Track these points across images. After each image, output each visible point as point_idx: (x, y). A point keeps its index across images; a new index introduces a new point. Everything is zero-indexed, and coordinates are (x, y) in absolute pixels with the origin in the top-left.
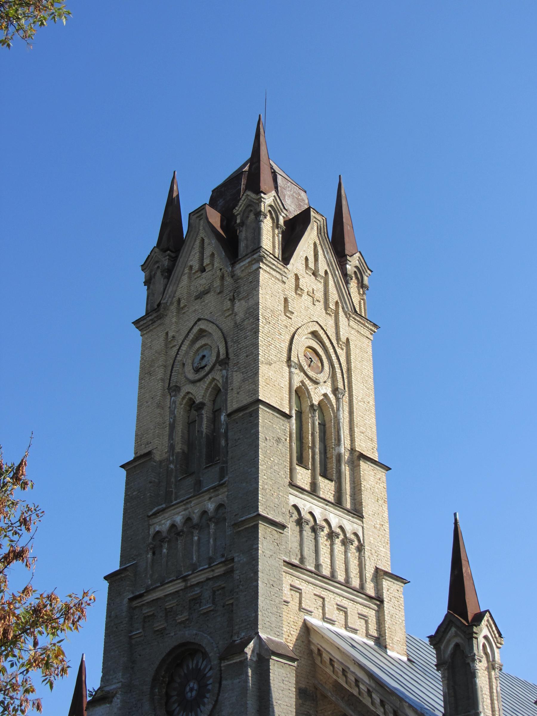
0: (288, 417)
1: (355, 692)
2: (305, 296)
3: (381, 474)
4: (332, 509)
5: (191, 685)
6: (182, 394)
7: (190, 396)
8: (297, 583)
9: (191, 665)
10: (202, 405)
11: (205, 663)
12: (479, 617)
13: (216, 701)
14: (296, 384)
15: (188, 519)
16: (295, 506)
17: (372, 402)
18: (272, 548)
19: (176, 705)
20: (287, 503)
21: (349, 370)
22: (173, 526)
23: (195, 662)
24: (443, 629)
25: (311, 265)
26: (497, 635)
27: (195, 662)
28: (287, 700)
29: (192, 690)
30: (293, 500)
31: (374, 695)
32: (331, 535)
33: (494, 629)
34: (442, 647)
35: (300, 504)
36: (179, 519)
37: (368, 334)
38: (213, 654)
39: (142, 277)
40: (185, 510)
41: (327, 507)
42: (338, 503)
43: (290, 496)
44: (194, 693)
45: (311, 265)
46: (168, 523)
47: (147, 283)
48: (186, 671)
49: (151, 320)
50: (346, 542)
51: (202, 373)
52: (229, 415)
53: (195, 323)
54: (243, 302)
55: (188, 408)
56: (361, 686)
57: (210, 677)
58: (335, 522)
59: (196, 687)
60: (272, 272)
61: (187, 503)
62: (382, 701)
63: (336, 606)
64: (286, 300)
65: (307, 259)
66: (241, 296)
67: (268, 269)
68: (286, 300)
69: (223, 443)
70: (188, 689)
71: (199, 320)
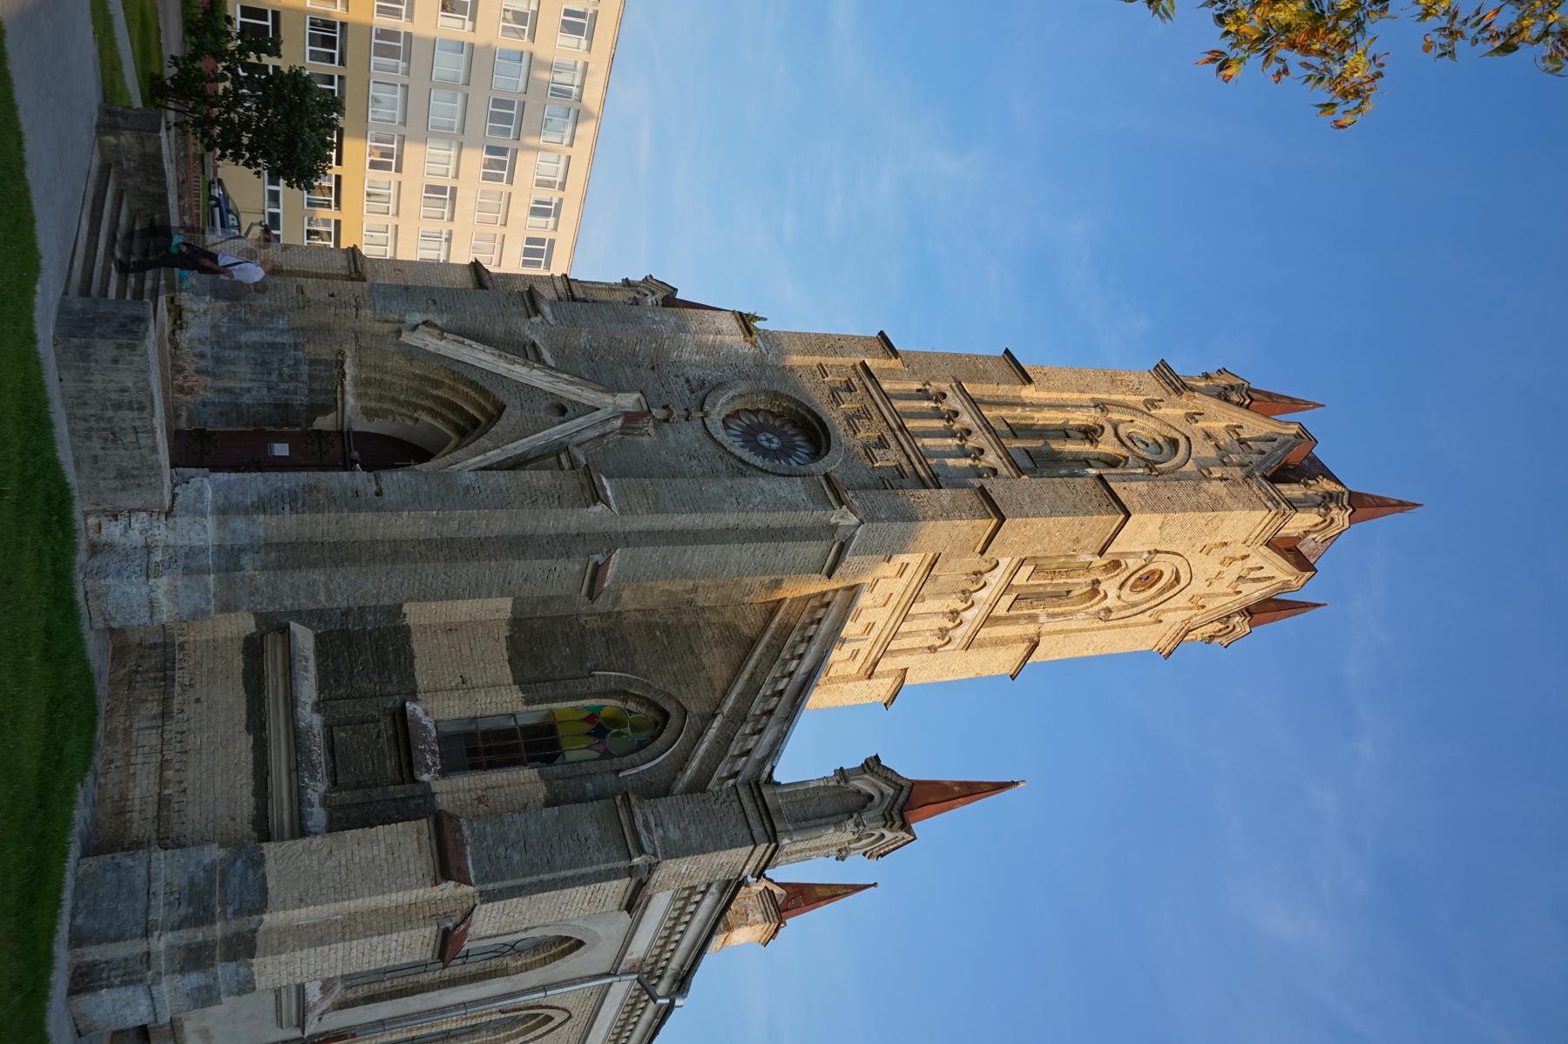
1: (785, 654)
2: (1218, 568)
3: (1009, 669)
4: (984, 611)
5: (775, 440)
7: (1100, 430)
8: (909, 572)
9: (799, 440)
11: (805, 456)
12: (905, 827)
13: (766, 471)
16: (997, 564)
17: (1086, 654)
18: (961, 537)
19: (761, 420)
20: (1003, 555)
21: (1127, 626)
23: (803, 444)
24: (890, 775)
26: (882, 852)
27: (803, 444)
28: (781, 564)
29: (769, 440)
30: (1004, 562)
31: (786, 680)
32: (954, 614)
33: (891, 847)
34: (866, 776)
35: (998, 572)
37: (1160, 645)
38: (819, 467)
40: (978, 426)
41: (987, 606)
42: (989, 620)
43: (1010, 558)
44: (766, 444)
45: (1253, 575)
48: (790, 433)
49: (1171, 381)
50: (943, 632)
51: (1129, 443)
52: (1100, 477)
53: (1183, 434)
54: (1225, 491)
55: (1083, 428)
56: (795, 663)
57: (789, 464)
58: (968, 615)
59: (774, 446)
60: (1263, 525)
61: (987, 429)
62: (781, 693)
63: (872, 621)
66: (1232, 489)
67: (1266, 521)
69: (1063, 472)
70: (769, 436)
71: (1188, 439)
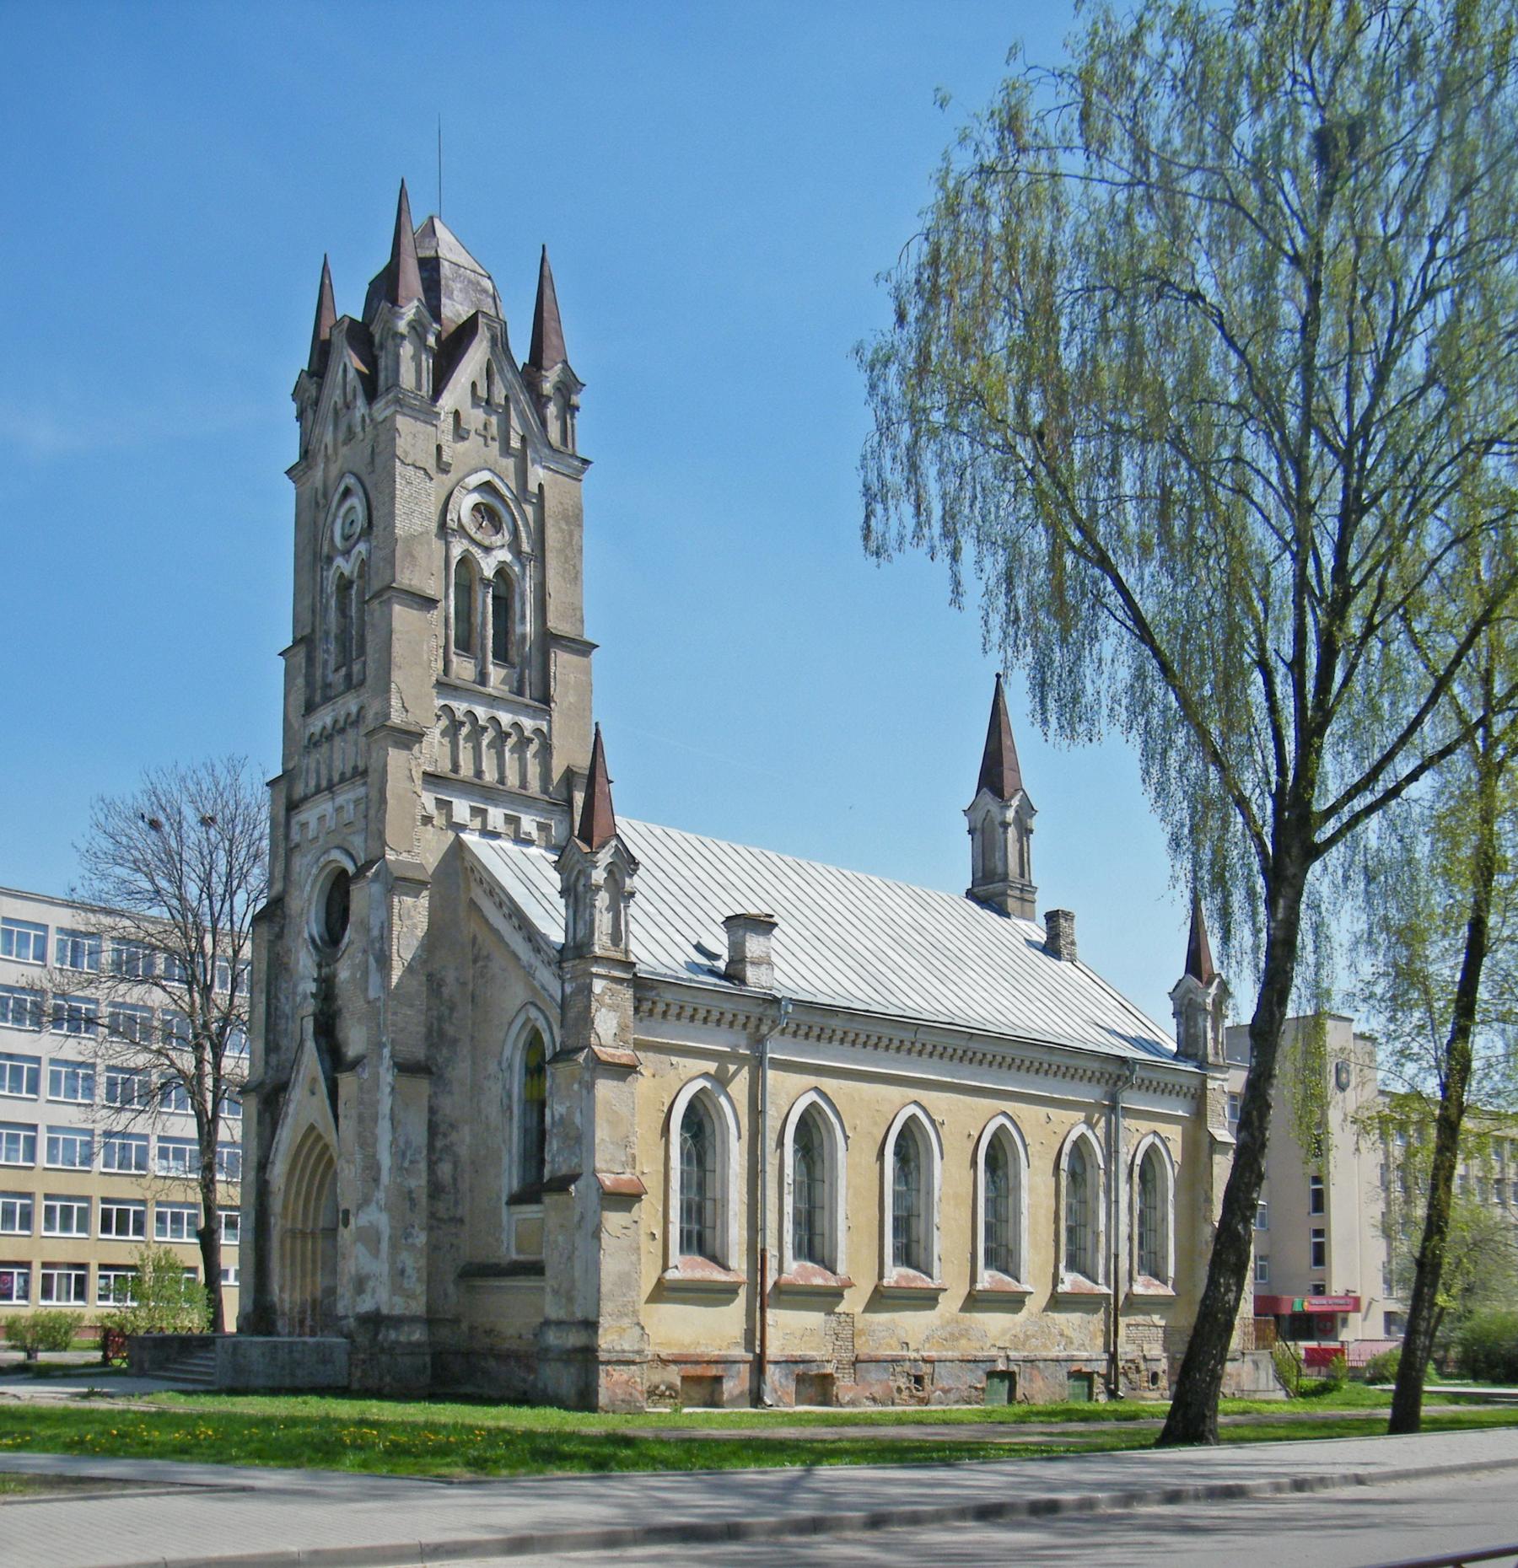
0: (429, 603)
6: (335, 564)
10: (351, 583)
14: (456, 552)
15: (336, 722)
22: (324, 728)
25: (482, 392)
36: (329, 721)
39: (292, 408)
45: (482, 392)
46: (320, 725)
47: (300, 417)
64: (439, 448)
65: (474, 385)
68: (439, 448)
